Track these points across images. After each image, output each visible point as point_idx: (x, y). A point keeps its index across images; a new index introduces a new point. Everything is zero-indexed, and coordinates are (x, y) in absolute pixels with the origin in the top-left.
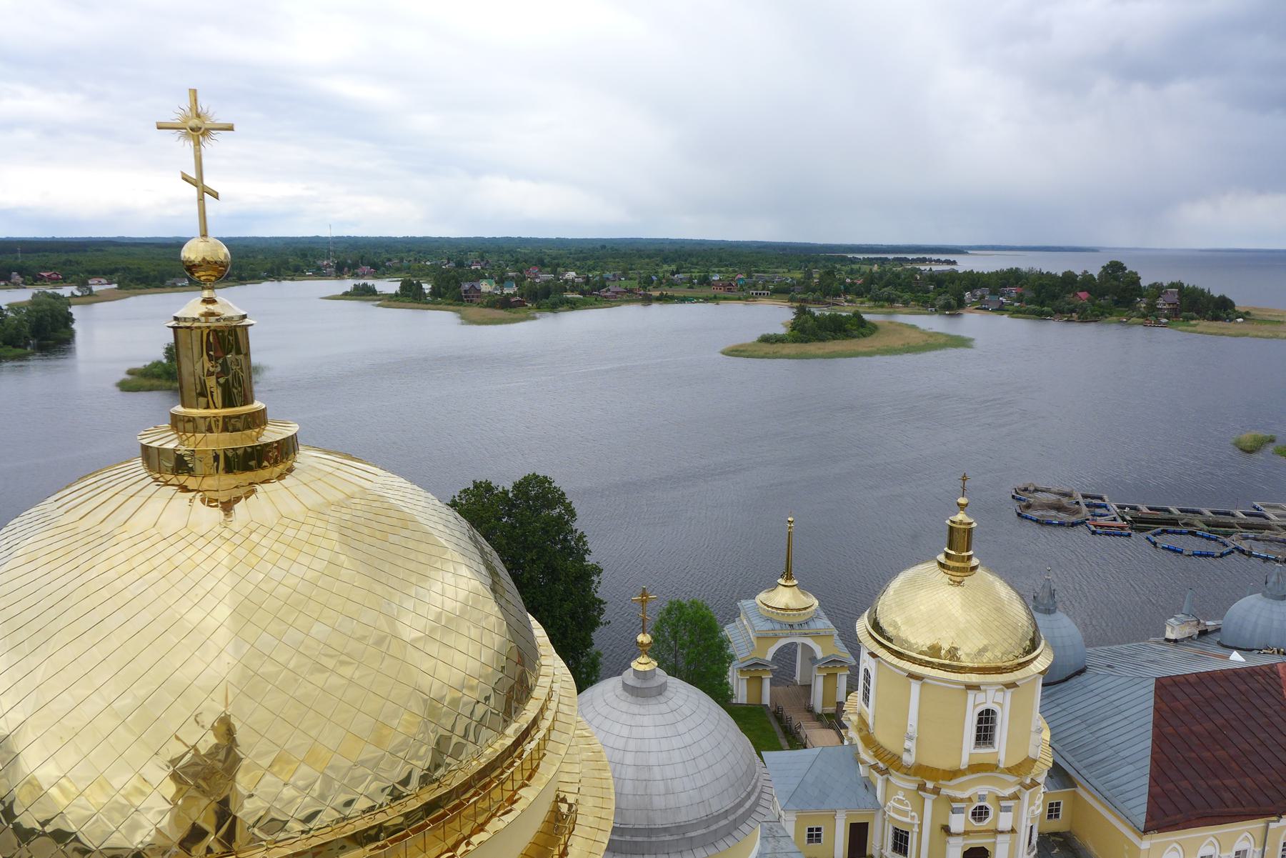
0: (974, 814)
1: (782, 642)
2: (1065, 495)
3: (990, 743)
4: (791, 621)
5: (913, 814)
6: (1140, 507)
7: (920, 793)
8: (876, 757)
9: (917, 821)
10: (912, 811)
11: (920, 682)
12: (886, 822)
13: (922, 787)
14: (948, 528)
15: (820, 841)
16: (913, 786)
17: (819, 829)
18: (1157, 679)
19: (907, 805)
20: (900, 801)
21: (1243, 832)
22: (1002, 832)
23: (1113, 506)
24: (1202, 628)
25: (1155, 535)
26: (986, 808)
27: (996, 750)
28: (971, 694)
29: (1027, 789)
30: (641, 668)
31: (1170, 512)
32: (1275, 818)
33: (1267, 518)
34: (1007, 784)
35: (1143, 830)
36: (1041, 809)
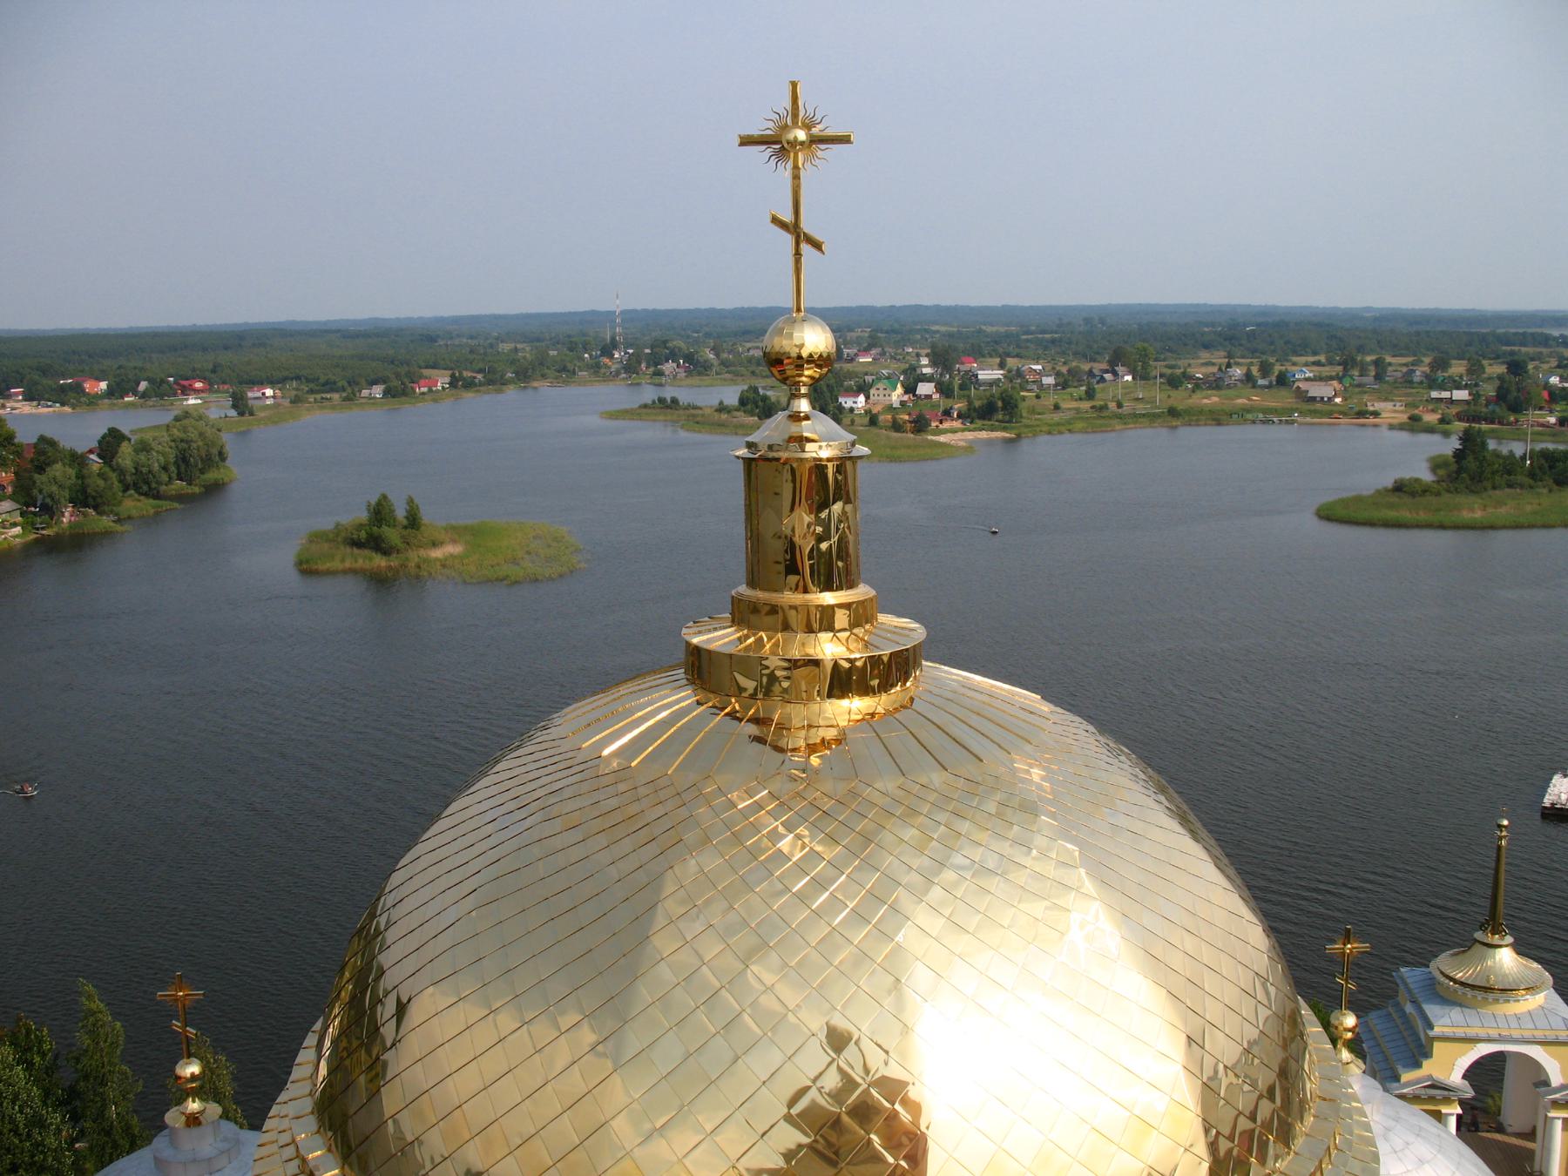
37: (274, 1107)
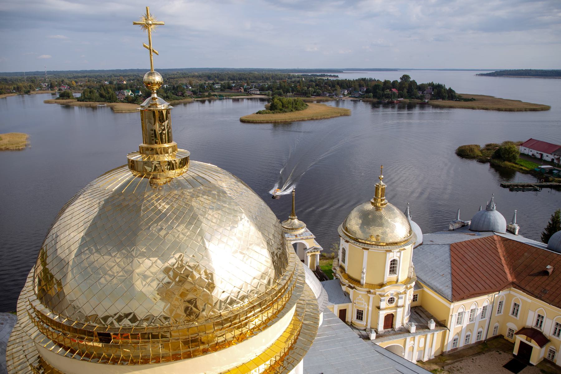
0: (389, 301)
3: (395, 273)
7: (368, 294)
10: (365, 302)
11: (367, 251)
12: (354, 308)
13: (369, 292)
14: (375, 188)
18: (451, 245)
26: (393, 298)
32: (497, 293)
37: (18, 300)
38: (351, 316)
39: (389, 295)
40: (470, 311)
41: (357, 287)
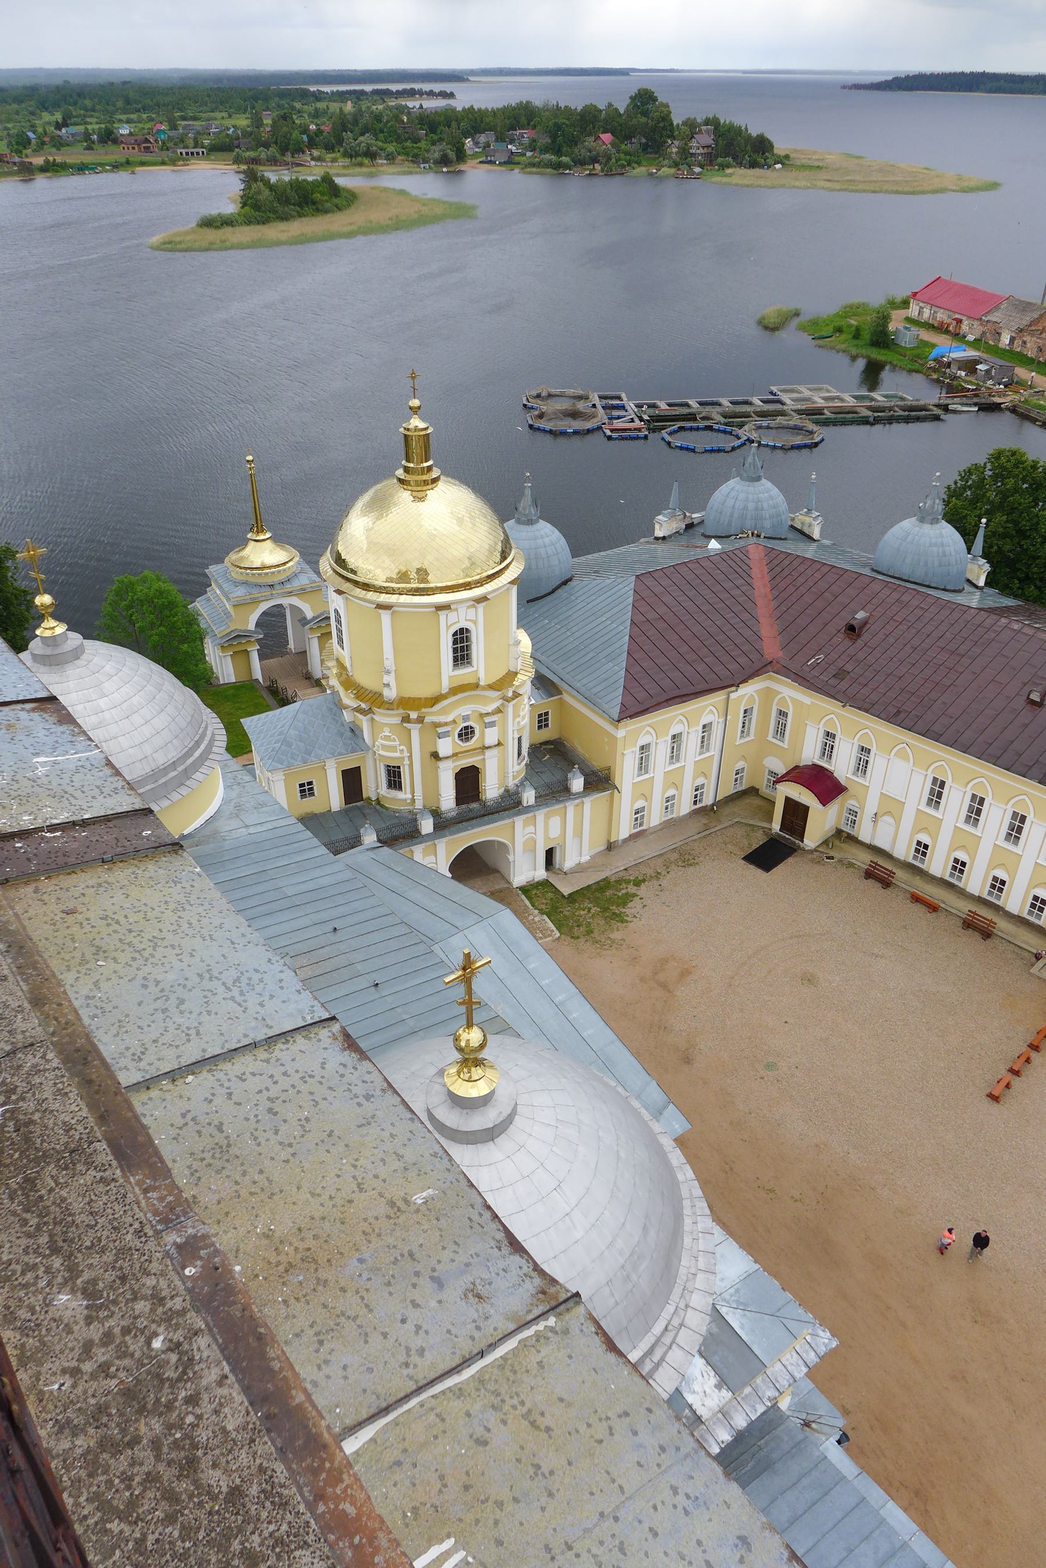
0: (460, 735)
1: (264, 606)
2: (580, 398)
3: (468, 663)
4: (269, 580)
5: (402, 747)
6: (659, 403)
8: (357, 698)
9: (406, 754)
11: (389, 612)
13: (406, 719)
15: (313, 794)
16: (397, 720)
17: (310, 783)
19: (394, 740)
20: (387, 738)
21: (707, 706)
22: (487, 748)
23: (631, 405)
24: (688, 521)
25: (670, 434)
27: (475, 668)
28: (442, 615)
29: (508, 701)
30: (48, 633)
31: (687, 405)
32: (733, 688)
33: (783, 404)
34: (486, 700)
35: (616, 718)
36: (527, 720)
38: (374, 784)
39: (459, 721)
40: (670, 737)
41: (375, 709)
